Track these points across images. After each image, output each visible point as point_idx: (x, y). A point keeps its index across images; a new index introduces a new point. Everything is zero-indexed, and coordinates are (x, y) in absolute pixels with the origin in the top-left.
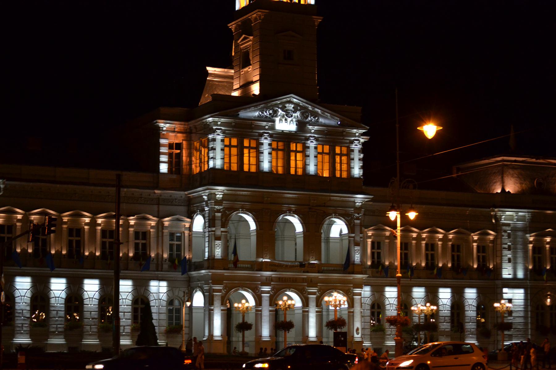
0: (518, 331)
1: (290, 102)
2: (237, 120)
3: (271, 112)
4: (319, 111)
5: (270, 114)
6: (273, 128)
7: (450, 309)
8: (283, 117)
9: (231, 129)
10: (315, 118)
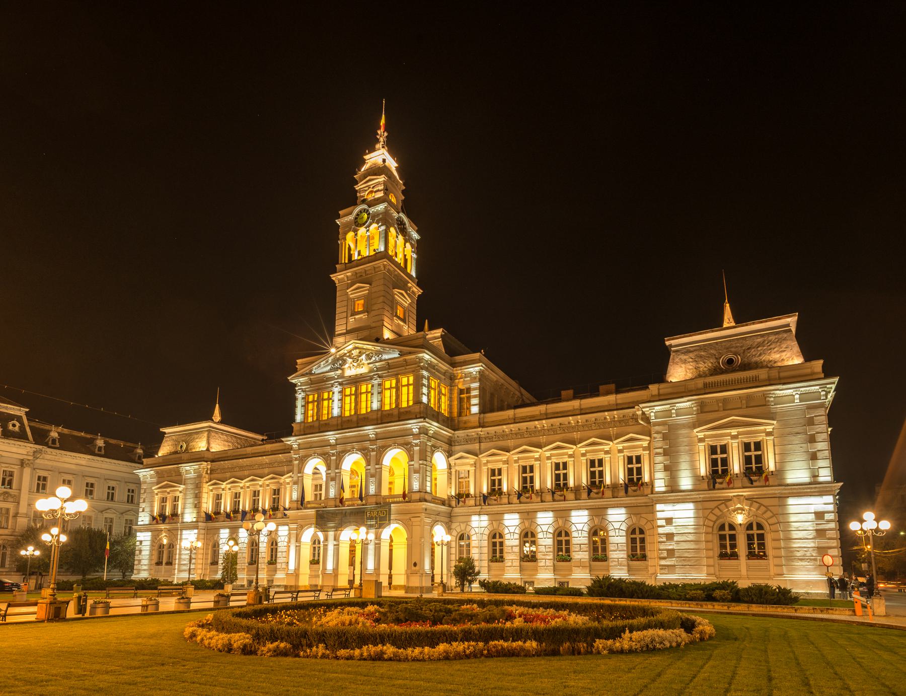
0: (683, 560)
1: (356, 348)
2: (311, 377)
3: (340, 362)
4: (379, 348)
5: (340, 364)
6: (342, 376)
7: (587, 535)
8: (351, 363)
9: (309, 386)
10: (378, 356)
